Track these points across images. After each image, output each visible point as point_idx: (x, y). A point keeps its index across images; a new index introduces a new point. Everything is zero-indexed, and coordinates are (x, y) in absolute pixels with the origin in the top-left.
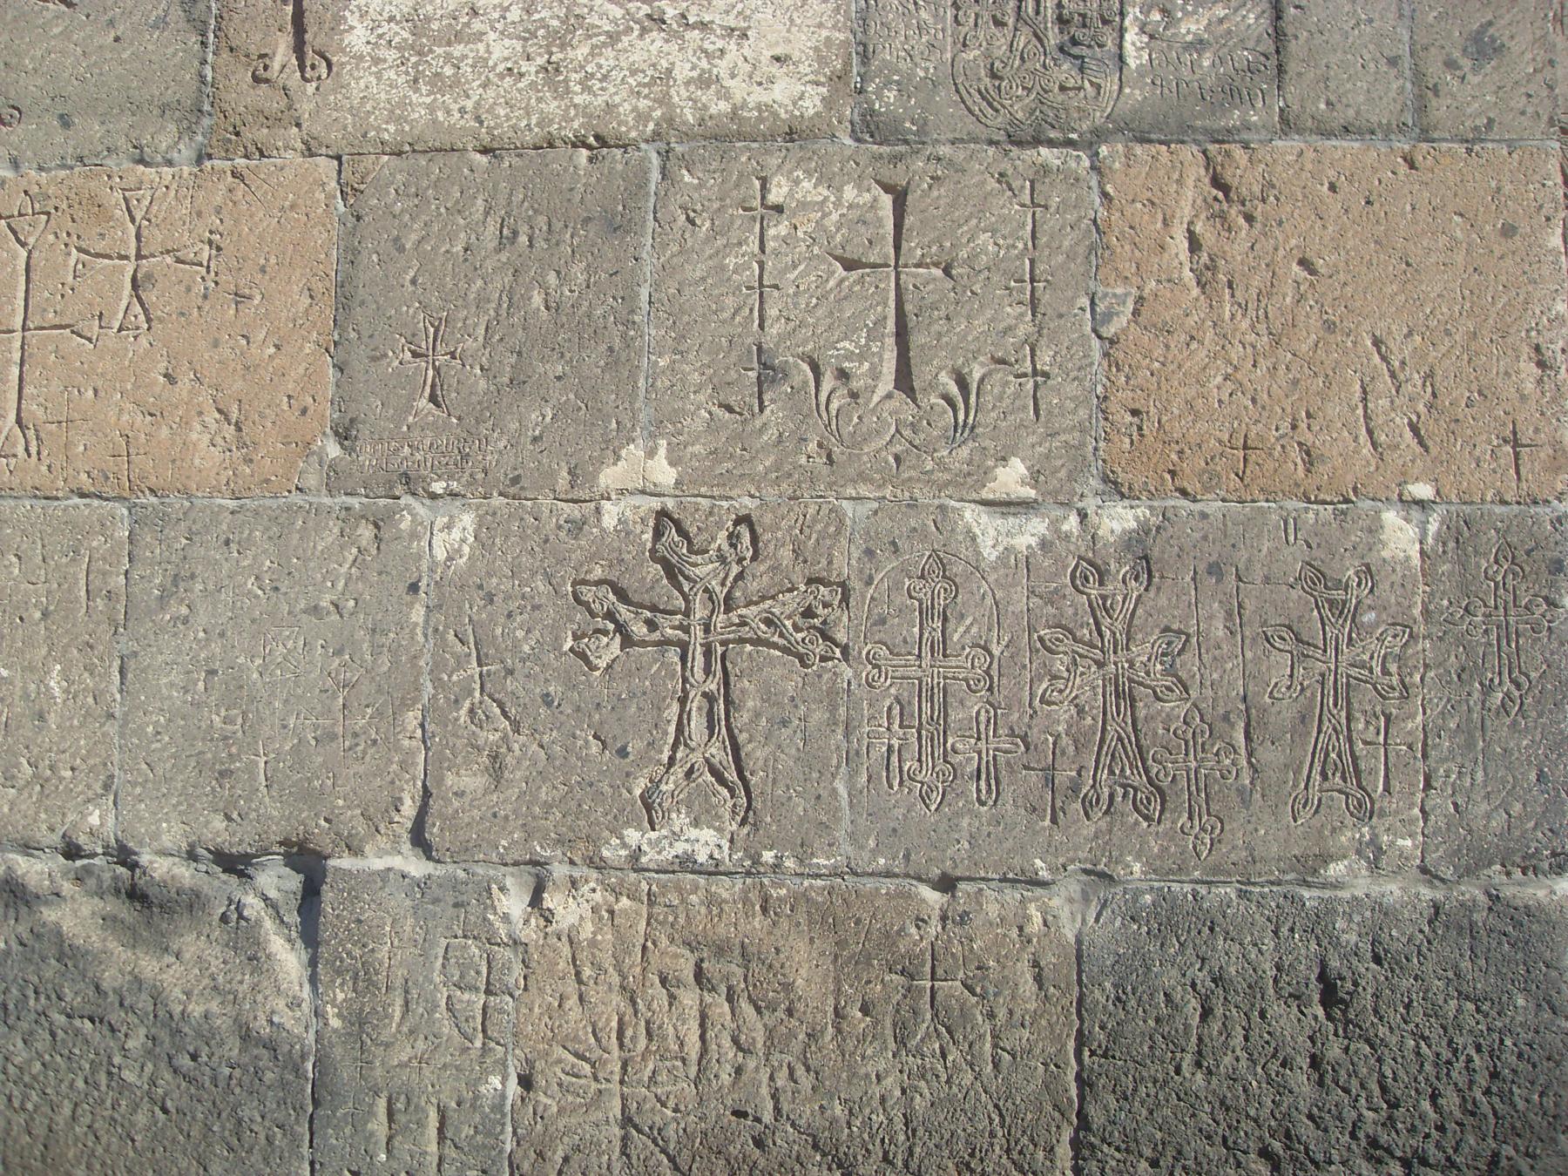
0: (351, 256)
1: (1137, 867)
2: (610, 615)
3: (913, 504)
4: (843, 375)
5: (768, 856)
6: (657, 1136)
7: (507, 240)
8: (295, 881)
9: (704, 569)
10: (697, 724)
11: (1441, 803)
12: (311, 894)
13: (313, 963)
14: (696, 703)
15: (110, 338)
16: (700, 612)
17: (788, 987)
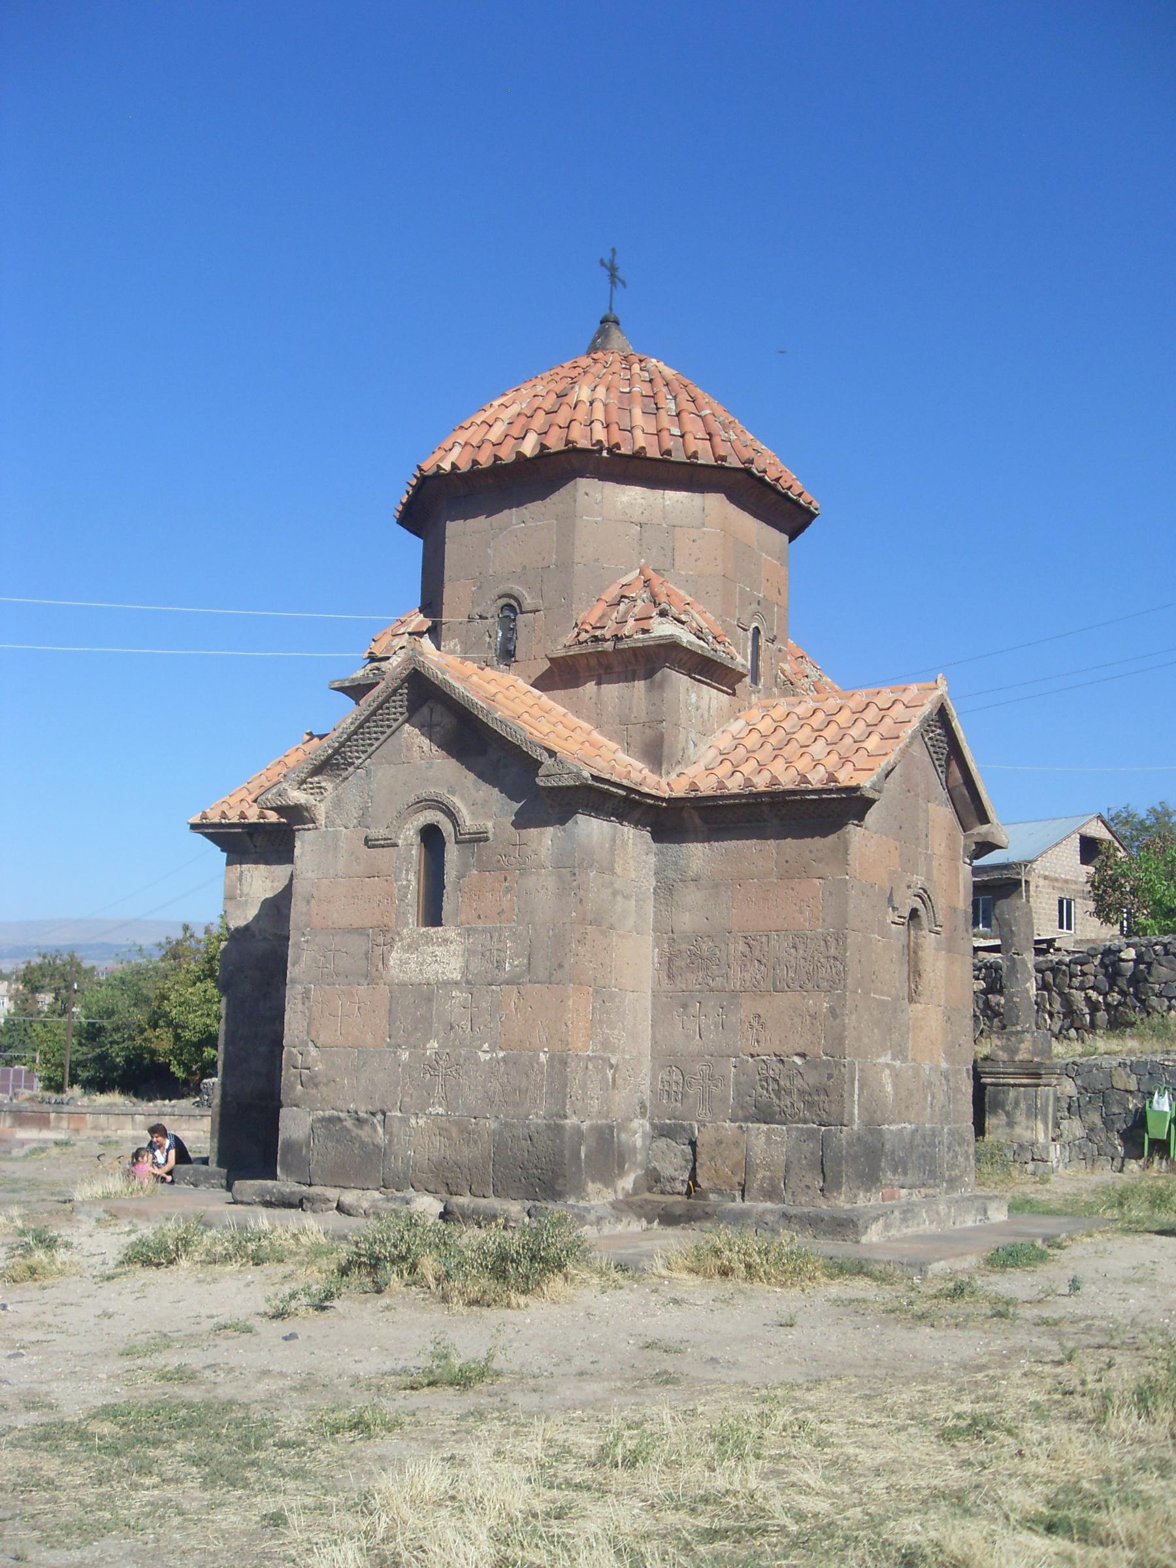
0: (391, 1004)
6: (432, 1162)
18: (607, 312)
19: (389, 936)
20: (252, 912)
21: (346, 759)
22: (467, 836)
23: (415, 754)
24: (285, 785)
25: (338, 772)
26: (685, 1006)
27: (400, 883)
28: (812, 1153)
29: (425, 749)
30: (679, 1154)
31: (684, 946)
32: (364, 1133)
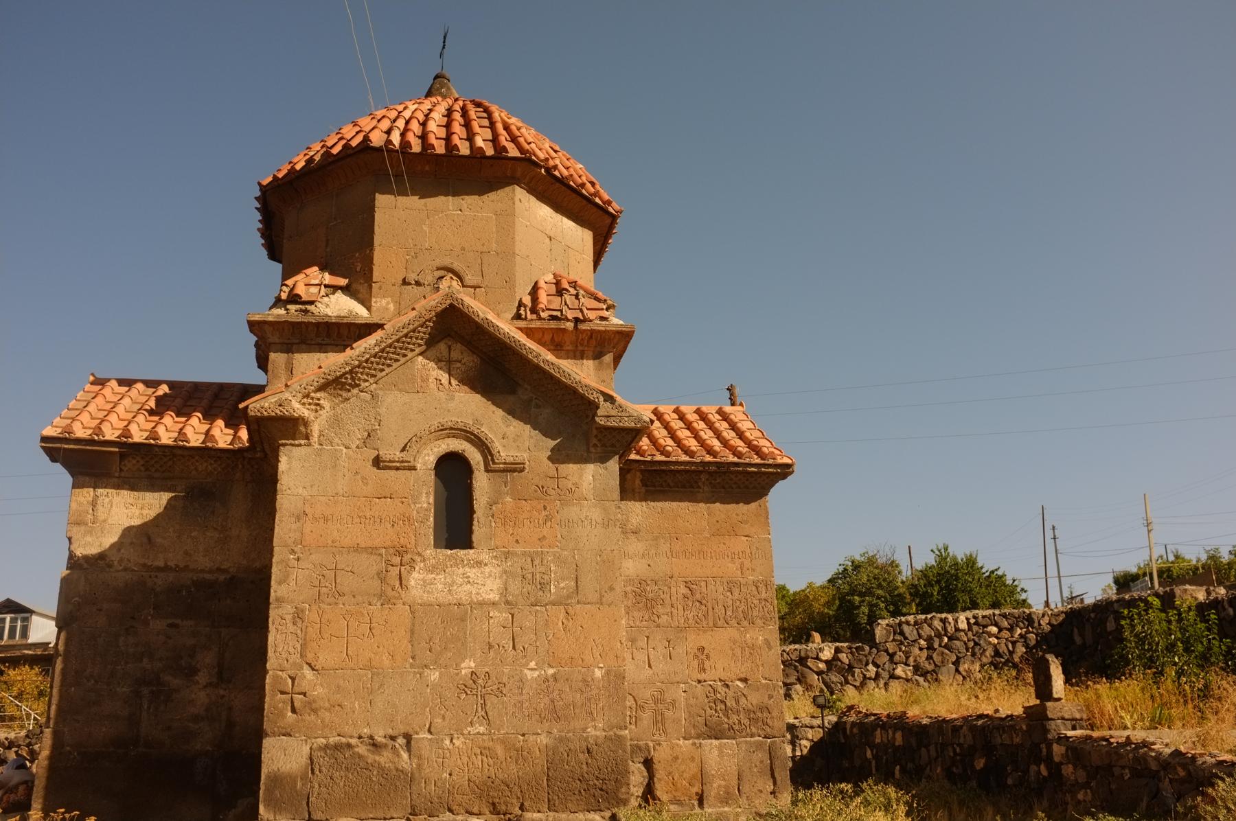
1: (556, 731)
2: (464, 690)
3: (516, 669)
4: (503, 647)
5: (493, 731)
6: (474, 782)
7: (442, 622)
8: (405, 741)
9: (480, 681)
10: (480, 709)
11: (605, 718)
12: (408, 743)
13: (410, 755)
14: (479, 705)
15: (366, 639)
16: (480, 689)
17: (497, 754)
18: (440, 71)
19: (409, 556)
20: (110, 539)
21: (354, 382)
22: (501, 466)
23: (432, 385)
24: (287, 395)
25: (340, 392)
26: (633, 641)
27: (417, 506)
28: (762, 762)
29: (443, 382)
30: (636, 772)
31: (629, 589)
32: (384, 758)
